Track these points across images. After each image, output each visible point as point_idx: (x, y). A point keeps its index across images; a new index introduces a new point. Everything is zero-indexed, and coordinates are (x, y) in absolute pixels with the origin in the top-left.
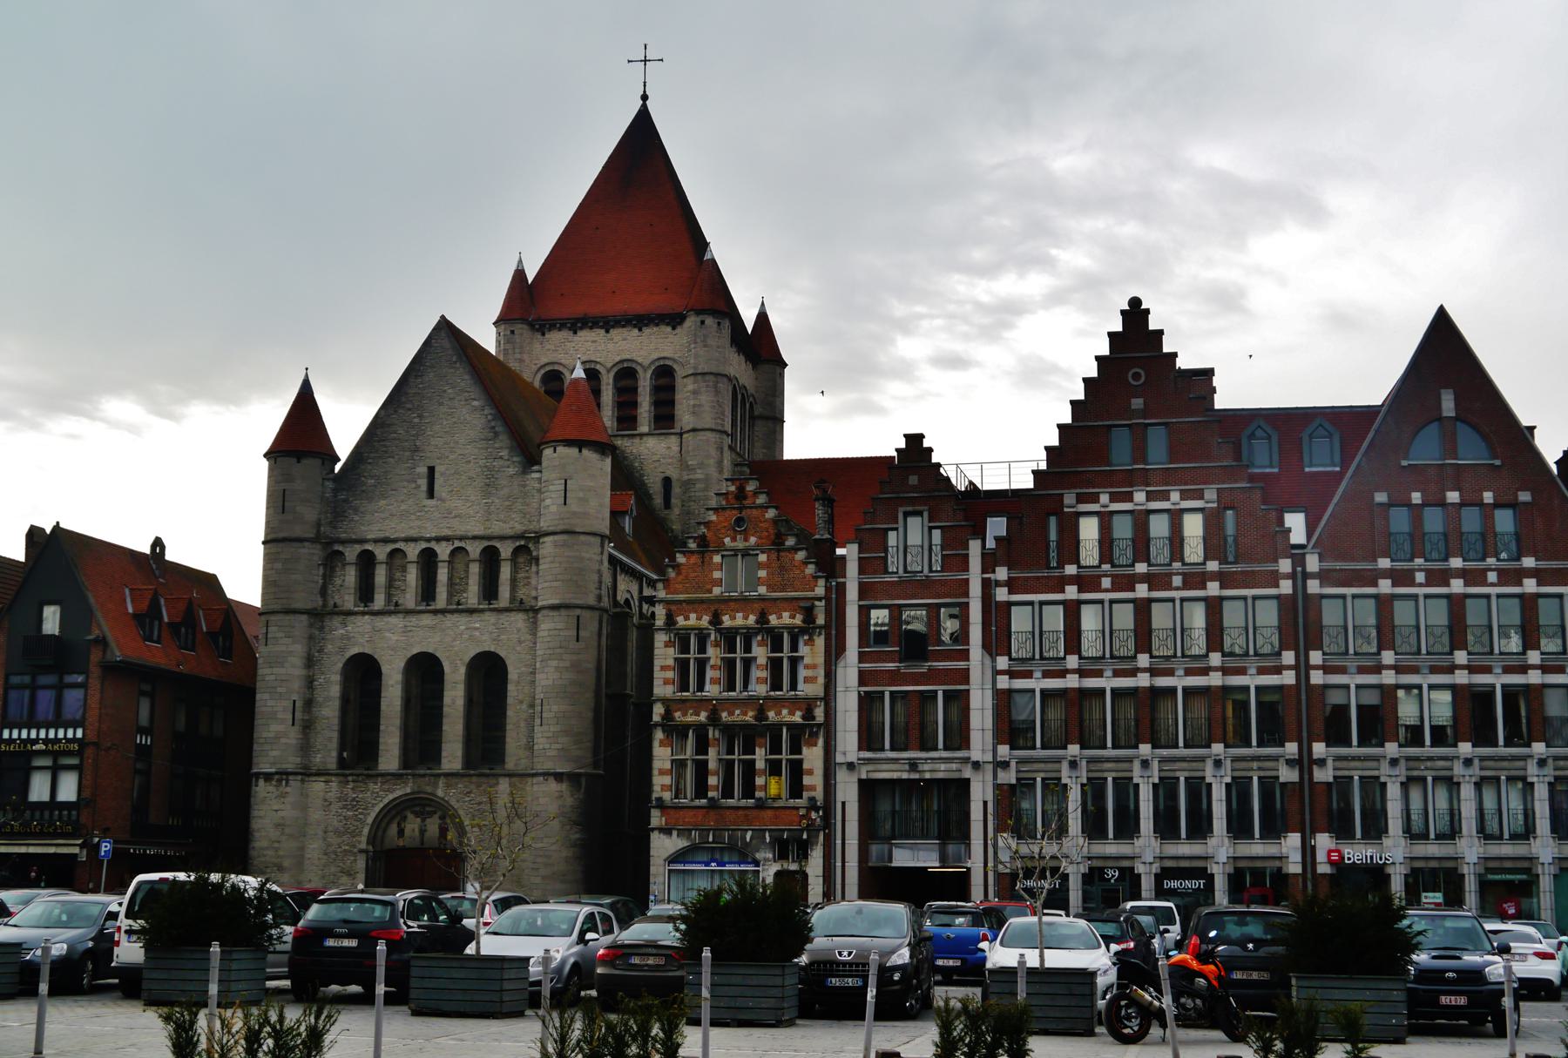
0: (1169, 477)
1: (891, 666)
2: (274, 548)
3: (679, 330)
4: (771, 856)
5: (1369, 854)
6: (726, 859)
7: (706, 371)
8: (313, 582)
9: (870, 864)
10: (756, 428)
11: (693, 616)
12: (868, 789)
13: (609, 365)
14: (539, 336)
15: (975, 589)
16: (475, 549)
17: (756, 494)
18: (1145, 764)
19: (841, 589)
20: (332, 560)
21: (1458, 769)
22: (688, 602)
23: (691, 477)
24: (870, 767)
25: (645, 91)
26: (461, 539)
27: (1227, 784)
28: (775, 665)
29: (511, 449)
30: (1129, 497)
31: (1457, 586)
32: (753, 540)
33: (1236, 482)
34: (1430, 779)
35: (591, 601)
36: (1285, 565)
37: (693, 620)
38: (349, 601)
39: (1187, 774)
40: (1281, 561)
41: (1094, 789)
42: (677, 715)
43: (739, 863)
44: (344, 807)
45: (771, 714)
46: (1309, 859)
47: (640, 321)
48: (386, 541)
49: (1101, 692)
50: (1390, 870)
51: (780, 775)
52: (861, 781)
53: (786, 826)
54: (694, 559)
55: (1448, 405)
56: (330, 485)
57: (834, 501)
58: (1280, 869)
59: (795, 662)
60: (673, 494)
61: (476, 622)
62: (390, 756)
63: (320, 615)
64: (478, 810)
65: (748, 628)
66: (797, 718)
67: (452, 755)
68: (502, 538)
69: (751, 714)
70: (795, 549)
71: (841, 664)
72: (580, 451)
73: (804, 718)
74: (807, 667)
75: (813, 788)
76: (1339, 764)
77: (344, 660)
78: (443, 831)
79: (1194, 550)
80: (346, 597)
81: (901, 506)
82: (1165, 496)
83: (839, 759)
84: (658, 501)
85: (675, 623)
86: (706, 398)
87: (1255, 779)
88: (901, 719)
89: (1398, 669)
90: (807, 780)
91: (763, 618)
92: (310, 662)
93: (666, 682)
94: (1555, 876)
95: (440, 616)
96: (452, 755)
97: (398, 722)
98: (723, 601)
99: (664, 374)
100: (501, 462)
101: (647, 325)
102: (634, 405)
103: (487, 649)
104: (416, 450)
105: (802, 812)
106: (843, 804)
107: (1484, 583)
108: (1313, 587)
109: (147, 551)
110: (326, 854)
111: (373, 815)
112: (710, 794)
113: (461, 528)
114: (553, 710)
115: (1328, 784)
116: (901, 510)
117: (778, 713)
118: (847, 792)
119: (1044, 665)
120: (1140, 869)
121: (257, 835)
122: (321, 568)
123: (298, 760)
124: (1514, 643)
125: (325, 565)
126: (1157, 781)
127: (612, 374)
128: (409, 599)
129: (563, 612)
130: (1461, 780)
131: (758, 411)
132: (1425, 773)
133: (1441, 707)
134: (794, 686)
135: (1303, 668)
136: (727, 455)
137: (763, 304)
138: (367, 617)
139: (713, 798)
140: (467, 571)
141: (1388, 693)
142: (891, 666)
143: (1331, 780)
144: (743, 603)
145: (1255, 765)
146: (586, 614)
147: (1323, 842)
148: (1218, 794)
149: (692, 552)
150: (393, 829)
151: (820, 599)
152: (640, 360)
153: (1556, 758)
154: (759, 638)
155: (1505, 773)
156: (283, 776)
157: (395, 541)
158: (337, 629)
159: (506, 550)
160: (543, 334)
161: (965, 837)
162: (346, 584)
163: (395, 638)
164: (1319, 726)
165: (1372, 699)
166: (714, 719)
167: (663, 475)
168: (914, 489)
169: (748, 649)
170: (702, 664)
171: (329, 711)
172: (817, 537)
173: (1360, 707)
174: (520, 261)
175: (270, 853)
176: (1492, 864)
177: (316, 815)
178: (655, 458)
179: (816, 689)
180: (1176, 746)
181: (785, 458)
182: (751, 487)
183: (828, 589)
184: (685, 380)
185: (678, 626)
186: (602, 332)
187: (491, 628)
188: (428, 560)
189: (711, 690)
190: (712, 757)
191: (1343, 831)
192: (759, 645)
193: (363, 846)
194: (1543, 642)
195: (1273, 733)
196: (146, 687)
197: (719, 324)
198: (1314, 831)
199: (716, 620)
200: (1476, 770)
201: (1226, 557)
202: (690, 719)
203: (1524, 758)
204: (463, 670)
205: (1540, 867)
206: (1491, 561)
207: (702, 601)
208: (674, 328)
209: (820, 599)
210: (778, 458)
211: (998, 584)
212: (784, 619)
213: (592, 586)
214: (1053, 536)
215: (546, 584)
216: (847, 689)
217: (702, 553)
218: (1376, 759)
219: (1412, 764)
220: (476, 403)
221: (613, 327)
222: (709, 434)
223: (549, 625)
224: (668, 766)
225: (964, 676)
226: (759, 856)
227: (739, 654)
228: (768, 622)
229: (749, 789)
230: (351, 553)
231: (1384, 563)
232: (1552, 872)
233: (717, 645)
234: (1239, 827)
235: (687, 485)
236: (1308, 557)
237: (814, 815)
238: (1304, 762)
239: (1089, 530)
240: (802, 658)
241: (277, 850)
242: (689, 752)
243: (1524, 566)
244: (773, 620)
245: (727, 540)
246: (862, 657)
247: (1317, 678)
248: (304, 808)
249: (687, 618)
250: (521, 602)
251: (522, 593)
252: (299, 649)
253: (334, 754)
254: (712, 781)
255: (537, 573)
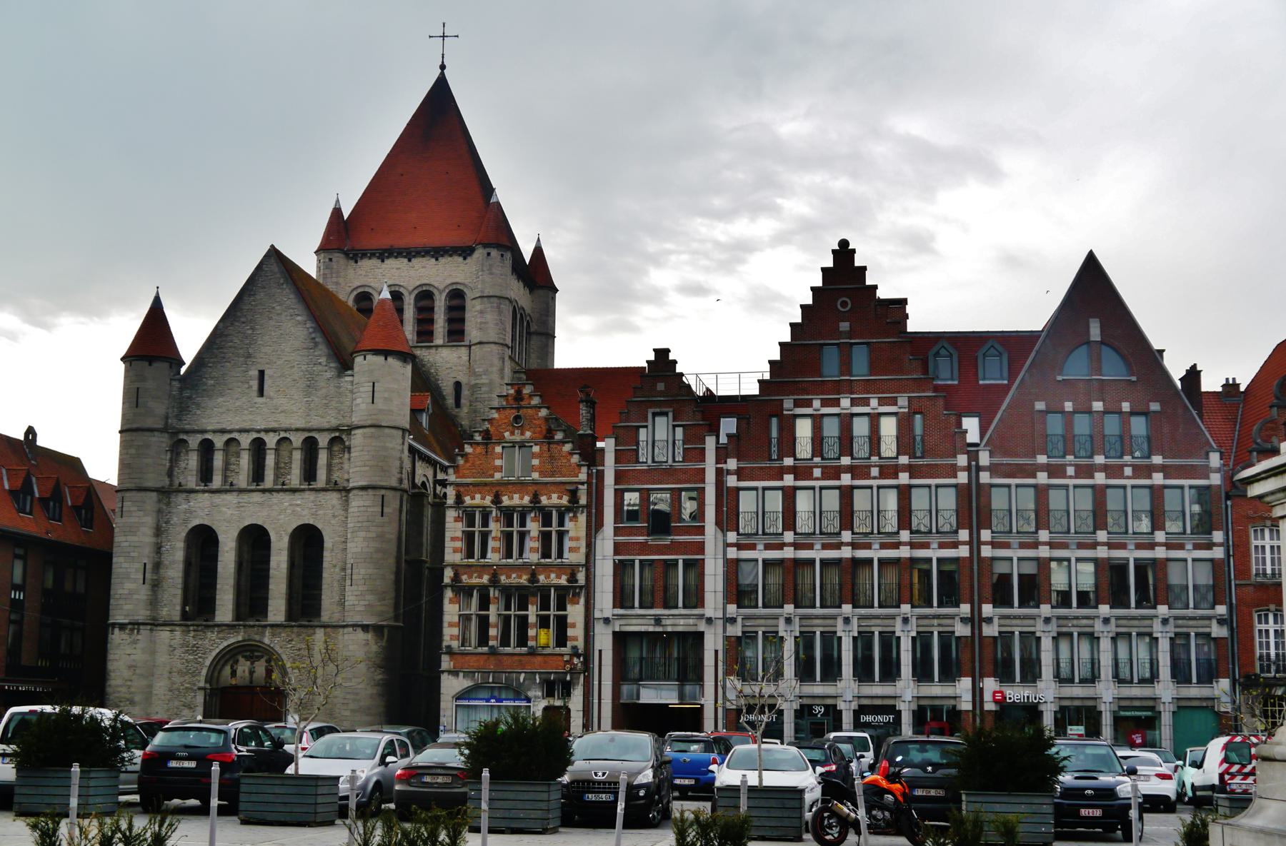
0: (869, 387)
1: (641, 539)
2: (128, 436)
3: (469, 260)
4: (540, 694)
5: (1026, 695)
6: (503, 696)
7: (491, 294)
8: (161, 465)
9: (621, 701)
10: (532, 342)
11: (478, 496)
12: (621, 639)
13: (411, 289)
14: (352, 263)
15: (710, 476)
16: (297, 440)
17: (531, 396)
18: (847, 620)
19: (600, 475)
20: (178, 447)
21: (1098, 627)
22: (475, 485)
23: (477, 381)
24: (623, 622)
25: (443, 62)
26: (286, 430)
27: (912, 637)
28: (545, 537)
29: (329, 356)
30: (836, 403)
31: (1100, 478)
32: (528, 434)
33: (924, 391)
34: (1075, 635)
35: (394, 483)
36: (962, 460)
37: (478, 500)
38: (191, 481)
39: (881, 629)
40: (959, 457)
41: (805, 641)
42: (464, 578)
43: (514, 700)
44: (187, 652)
45: (542, 578)
46: (978, 699)
47: (437, 252)
48: (223, 431)
49: (811, 562)
50: (1042, 708)
51: (548, 627)
52: (614, 633)
53: (554, 669)
54: (480, 449)
55: (1095, 332)
56: (176, 384)
57: (595, 403)
58: (954, 707)
59: (561, 535)
60: (462, 396)
61: (298, 499)
62: (225, 609)
63: (167, 493)
64: (298, 655)
65: (524, 507)
66: (563, 581)
67: (277, 609)
68: (320, 430)
69: (525, 577)
70: (563, 442)
71: (599, 537)
72: (386, 359)
73: (568, 581)
74: (571, 539)
75: (575, 639)
76: (1003, 622)
77: (187, 530)
78: (269, 672)
79: (889, 447)
80: (189, 478)
81: (651, 408)
82: (866, 402)
83: (597, 614)
84: (450, 401)
85: (463, 502)
86: (490, 317)
87: (936, 634)
88: (648, 583)
89: (1052, 545)
90: (570, 632)
91: (535, 499)
92: (158, 531)
93: (455, 550)
94: (1173, 712)
95: (267, 494)
96: (277, 609)
97: (231, 581)
98: (500, 484)
99: (457, 297)
100: (320, 368)
101: (442, 256)
102: (431, 321)
103: (307, 522)
104: (249, 356)
105: (566, 658)
106: (600, 651)
107: (1122, 476)
108: (985, 477)
109: (22, 438)
110: (170, 691)
111: (210, 659)
112: (491, 643)
113: (285, 421)
114: (361, 572)
115: (995, 638)
116: (650, 411)
117: (548, 577)
118: (604, 641)
119: (765, 539)
120: (841, 706)
121: (112, 674)
122: (169, 454)
123: (148, 613)
124: (1145, 525)
125: (172, 451)
126: (856, 635)
127: (413, 296)
128: (242, 480)
129: (371, 492)
130: (1101, 635)
131: (534, 328)
132: (1072, 629)
133: (1085, 577)
134: (560, 555)
135: (975, 543)
136: (508, 363)
137: (539, 240)
138: (206, 495)
139: (493, 647)
140: (290, 458)
141: (1044, 564)
142: (641, 539)
143: (996, 634)
144: (520, 486)
145: (936, 622)
146: (389, 494)
147: (990, 685)
148: (906, 645)
149: (478, 444)
150: (227, 670)
151: (582, 484)
152: (436, 284)
153: (1176, 618)
154: (533, 515)
155: (1136, 630)
156: (135, 625)
157: (230, 431)
158: (181, 504)
159: (323, 440)
160: (356, 262)
161: (700, 679)
162: (190, 467)
163: (230, 512)
164: (988, 592)
165: (1030, 569)
166: (494, 581)
167: (455, 380)
168: (661, 393)
169: (523, 524)
170: (485, 536)
171: (174, 573)
172: (581, 432)
173: (1020, 576)
174: (338, 201)
175: (123, 690)
176: (1124, 703)
177: (162, 658)
178: (448, 366)
179: (578, 557)
180: (872, 607)
181: (556, 367)
182: (527, 390)
183: (589, 475)
184: (474, 301)
185: (465, 505)
186: (406, 260)
187: (311, 505)
188: (258, 448)
189: (493, 557)
190: (493, 613)
191: (1005, 676)
192: (532, 521)
193: (202, 684)
194: (1168, 524)
195: (950, 596)
196: (20, 551)
197: (502, 255)
198: (982, 676)
199: (497, 500)
200: (1112, 627)
201: (914, 453)
202: (475, 581)
203: (1151, 618)
204: (286, 539)
205: (1162, 705)
206: (1127, 458)
207: (486, 484)
208: (465, 259)
209: (582, 484)
210: (551, 367)
211: (729, 472)
212: (552, 500)
213: (395, 471)
214: (774, 433)
215: (356, 469)
216: (604, 558)
217: (486, 444)
218: (1033, 618)
219: (1062, 622)
220: (299, 318)
221: (414, 257)
222: (493, 346)
223: (358, 502)
224: (456, 619)
225: (700, 548)
226: (530, 694)
227: (516, 528)
228: (539, 502)
229: (523, 641)
230: (194, 441)
231: (1042, 459)
232: (1172, 710)
233: (497, 520)
234: (922, 672)
235: (474, 388)
236: (981, 454)
237: (576, 661)
238: (975, 620)
239: (804, 429)
240: (568, 531)
241: (129, 687)
242: (474, 608)
243: (1154, 462)
244: (544, 500)
245: (507, 434)
246: (617, 531)
247: (986, 552)
248: (153, 653)
249: (473, 498)
250: (336, 483)
251: (336, 476)
252: (149, 520)
253: (178, 608)
254: (493, 632)
255: (349, 459)
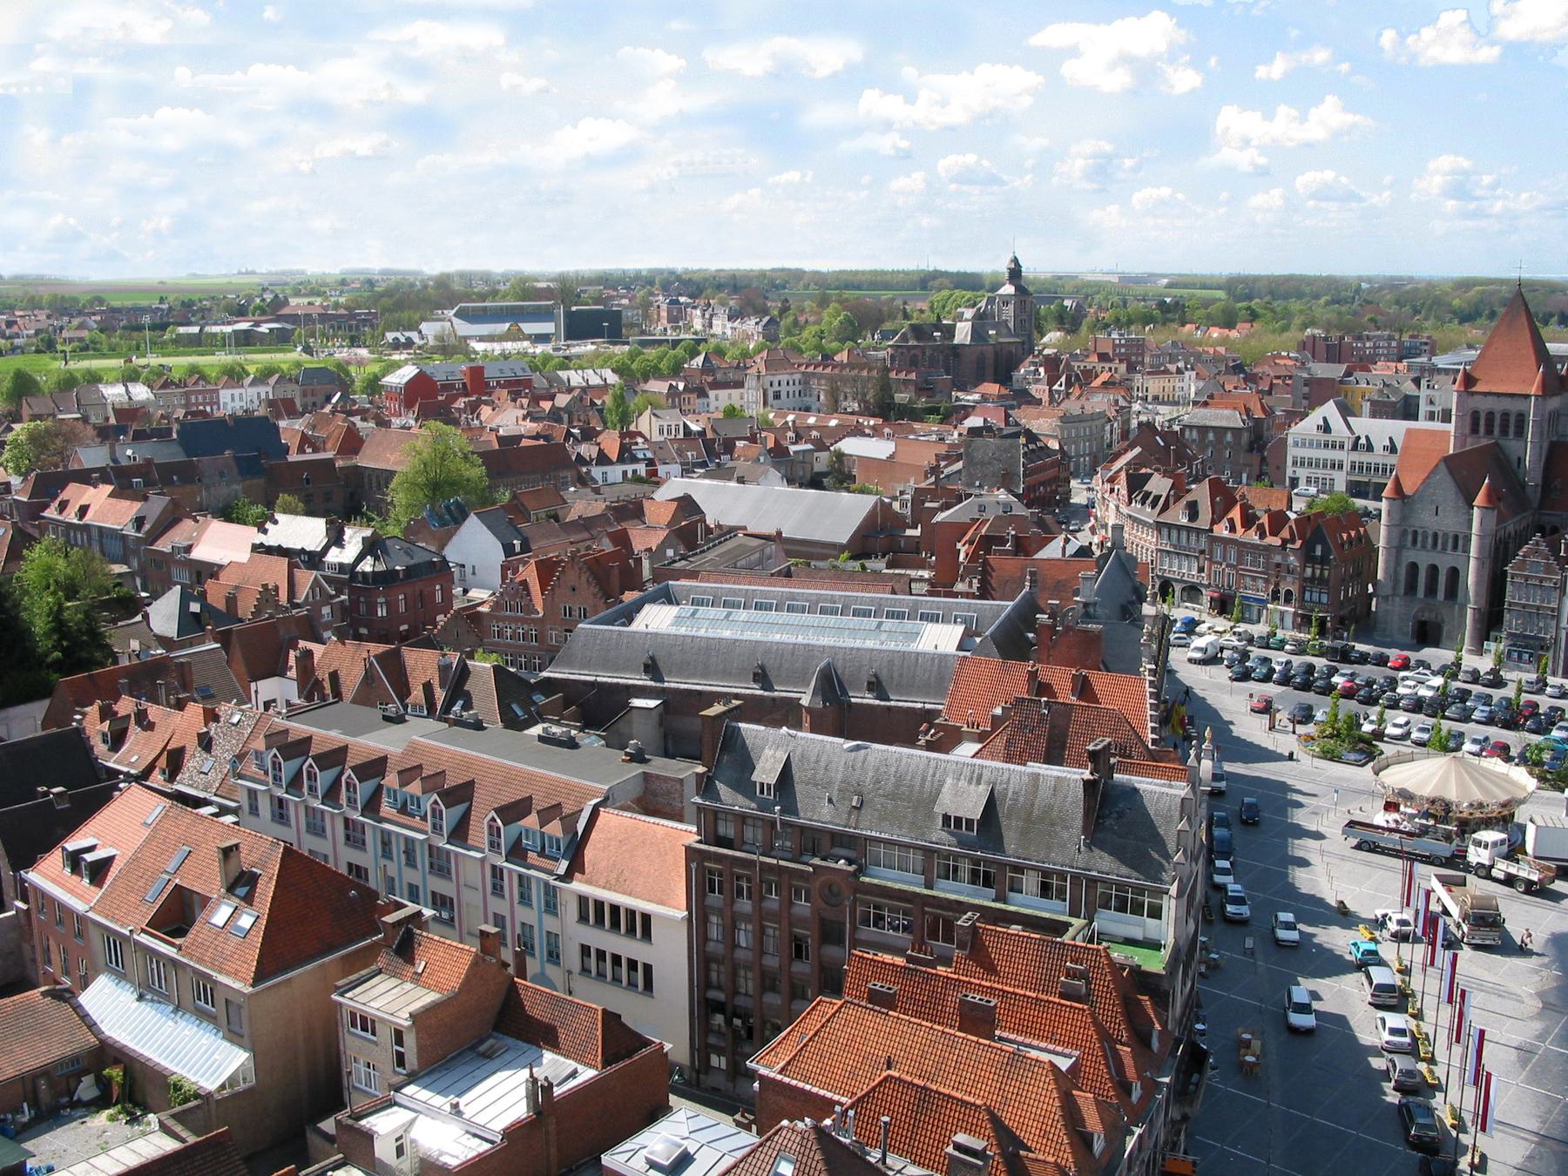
38: (1409, 544)
67: (1441, 595)
96: (1441, 595)
159: (1461, 536)
